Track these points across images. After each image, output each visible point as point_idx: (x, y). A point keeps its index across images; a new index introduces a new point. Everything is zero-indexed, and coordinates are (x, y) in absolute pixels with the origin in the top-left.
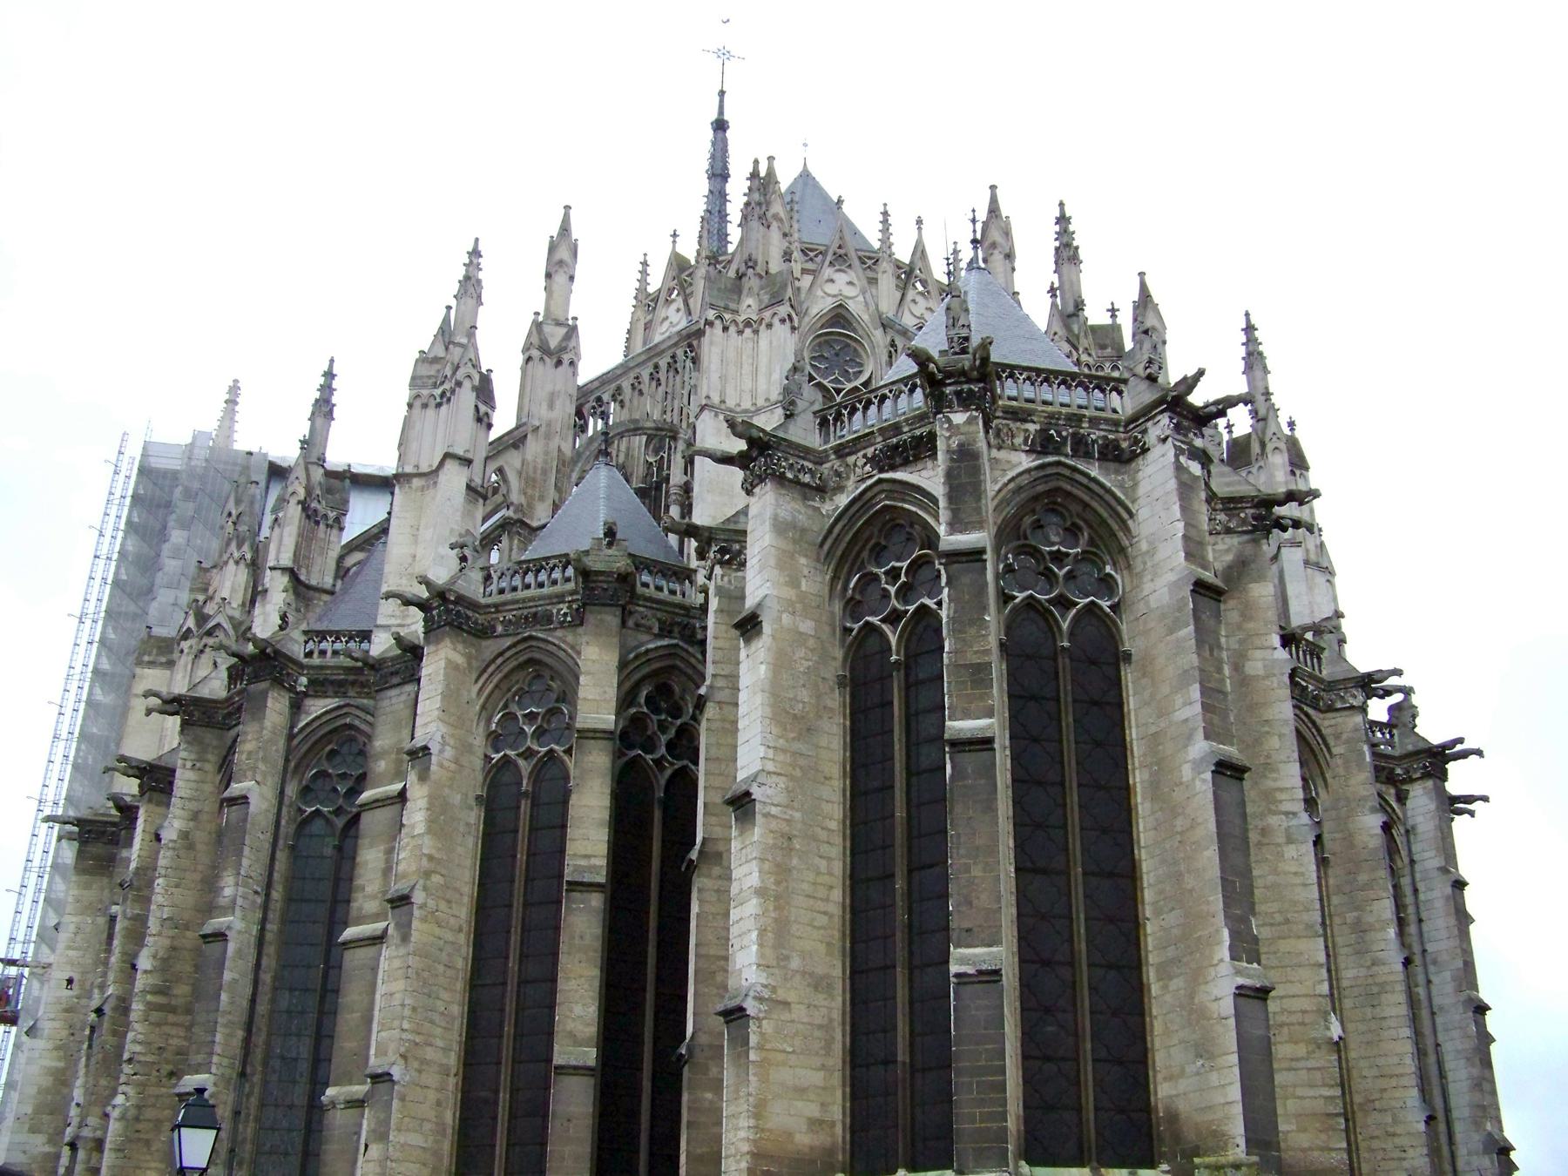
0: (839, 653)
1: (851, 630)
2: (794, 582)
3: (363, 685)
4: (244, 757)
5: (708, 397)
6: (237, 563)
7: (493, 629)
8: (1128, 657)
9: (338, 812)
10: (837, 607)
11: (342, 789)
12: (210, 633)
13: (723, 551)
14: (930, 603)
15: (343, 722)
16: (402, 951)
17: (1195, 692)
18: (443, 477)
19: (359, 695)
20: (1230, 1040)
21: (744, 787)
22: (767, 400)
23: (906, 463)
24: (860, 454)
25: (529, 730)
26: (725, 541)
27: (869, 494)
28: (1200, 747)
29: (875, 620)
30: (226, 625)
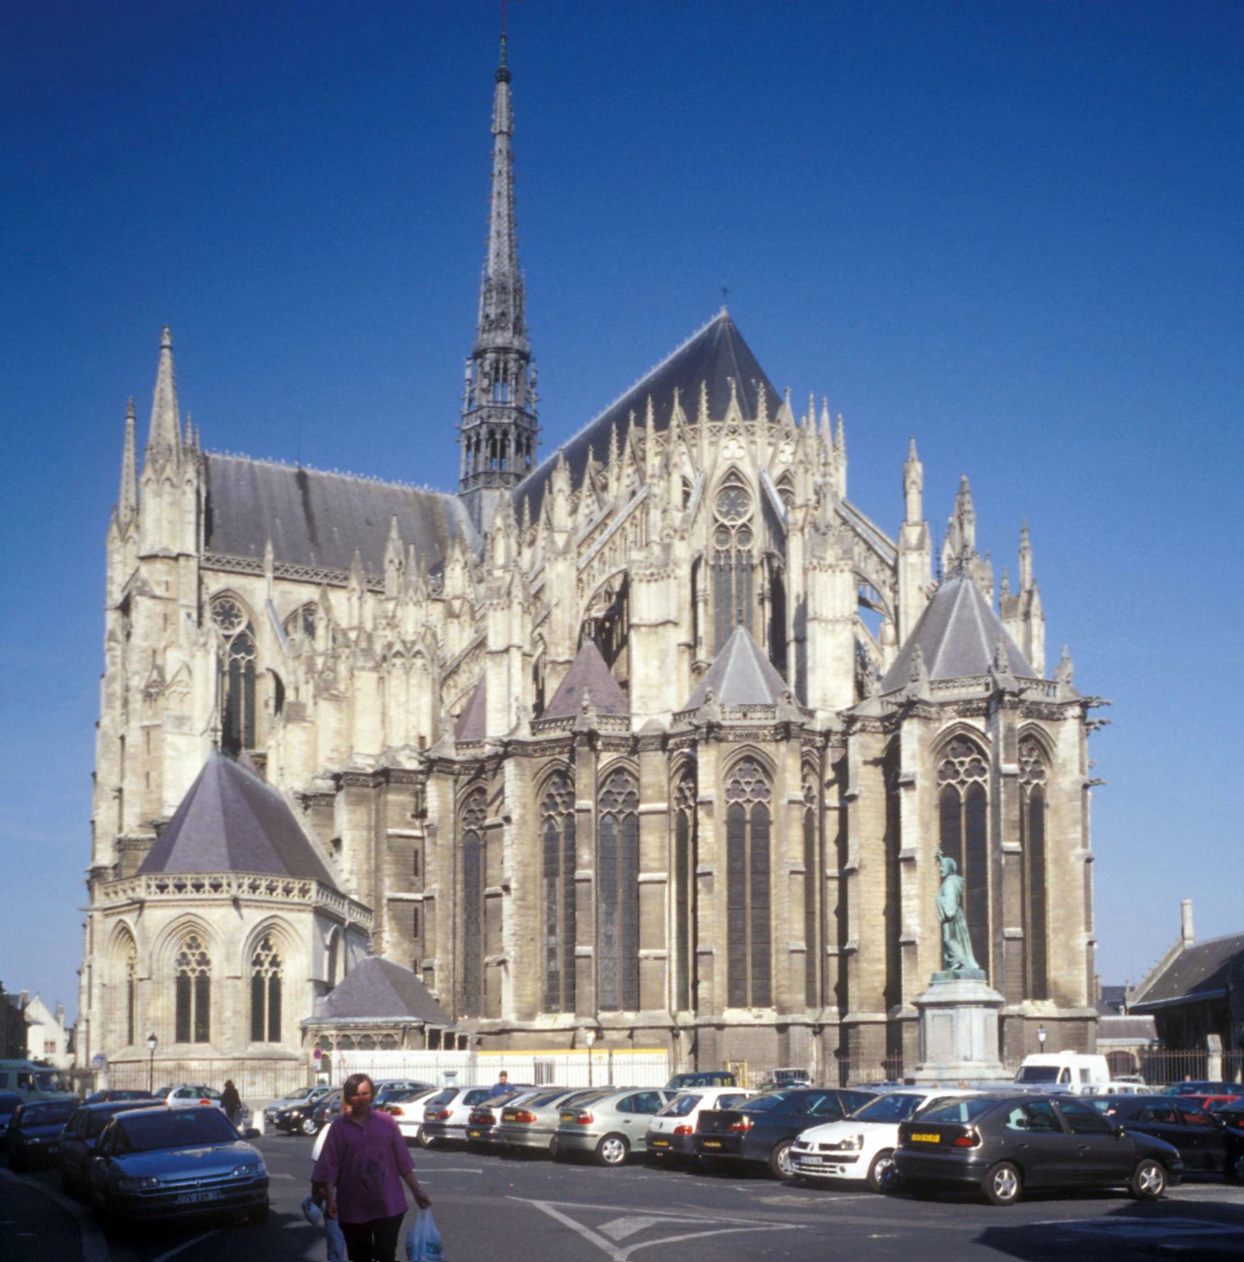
2: (923, 765)
8: (1047, 806)
12: (414, 656)
17: (1079, 828)
20: (1083, 958)
28: (1079, 850)
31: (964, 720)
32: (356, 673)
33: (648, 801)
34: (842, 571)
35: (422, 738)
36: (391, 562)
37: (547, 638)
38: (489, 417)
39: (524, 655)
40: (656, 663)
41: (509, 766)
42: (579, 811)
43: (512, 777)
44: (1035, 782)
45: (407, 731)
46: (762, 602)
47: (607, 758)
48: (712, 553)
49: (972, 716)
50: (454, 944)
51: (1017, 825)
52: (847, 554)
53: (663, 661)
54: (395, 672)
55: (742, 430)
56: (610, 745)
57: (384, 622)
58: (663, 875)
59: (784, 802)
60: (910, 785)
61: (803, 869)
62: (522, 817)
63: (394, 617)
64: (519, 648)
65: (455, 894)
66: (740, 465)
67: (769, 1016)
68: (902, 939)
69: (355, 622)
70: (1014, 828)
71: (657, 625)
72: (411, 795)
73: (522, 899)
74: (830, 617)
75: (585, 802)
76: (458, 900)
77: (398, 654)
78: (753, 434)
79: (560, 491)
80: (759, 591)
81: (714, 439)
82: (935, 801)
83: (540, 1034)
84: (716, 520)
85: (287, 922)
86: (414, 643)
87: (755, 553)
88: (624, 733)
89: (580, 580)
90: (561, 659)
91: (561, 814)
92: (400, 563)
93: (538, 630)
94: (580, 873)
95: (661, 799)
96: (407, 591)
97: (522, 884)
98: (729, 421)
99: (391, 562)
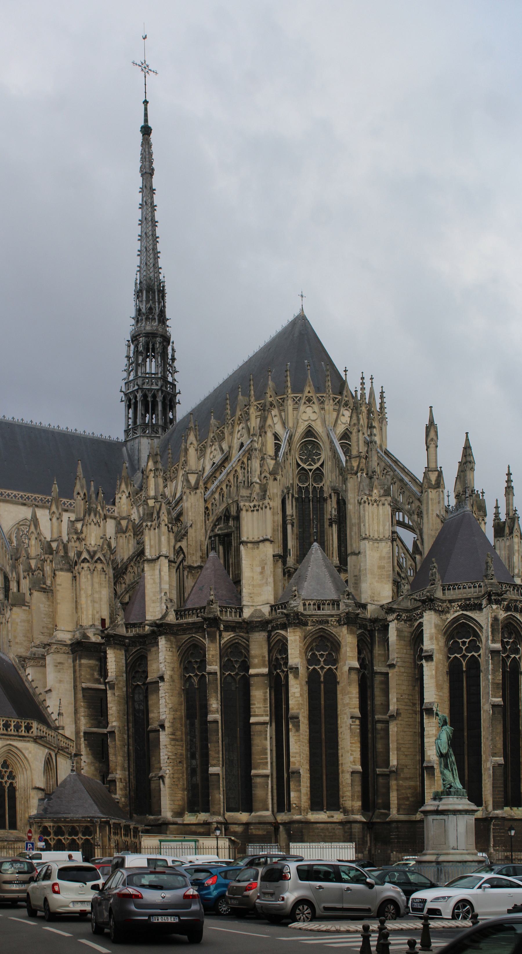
0: (447, 664)
1: (450, 657)
2: (438, 644)
3: (242, 628)
5: (366, 534)
6: (95, 524)
7: (308, 623)
9: (237, 674)
10: (446, 650)
11: (237, 666)
12: (96, 562)
13: (398, 615)
14: (476, 654)
15: (234, 642)
16: (297, 734)
19: (240, 632)
21: (430, 707)
22: (384, 537)
25: (322, 660)
26: (398, 612)
29: (458, 656)
30: (102, 558)
31: (465, 613)
32: (57, 573)
33: (255, 667)
35: (103, 621)
36: (78, 494)
37: (185, 550)
38: (143, 384)
39: (170, 561)
40: (259, 569)
41: (162, 642)
42: (210, 673)
43: (164, 649)
44: (513, 656)
45: (93, 615)
46: (331, 525)
47: (227, 636)
48: (296, 489)
49: (471, 610)
50: (129, 763)
51: (501, 686)
52: (387, 493)
53: (263, 568)
54: (83, 573)
55: (315, 400)
56: (230, 627)
57: (75, 537)
58: (267, 719)
59: (346, 668)
60: (429, 658)
61: (359, 715)
62: (171, 677)
63: (82, 532)
64: (166, 557)
65: (128, 730)
66: (313, 424)
67: (338, 816)
68: (425, 765)
69: (55, 536)
70: (498, 688)
71: (258, 542)
72: (97, 660)
73: (173, 734)
74: (376, 536)
75: (214, 667)
76: (130, 733)
77: (85, 560)
78: (323, 403)
79: (191, 444)
80: (329, 517)
81: (296, 406)
82: (446, 669)
83: (187, 827)
84: (299, 465)
85: (16, 747)
86: (95, 552)
87: (325, 489)
88: (238, 619)
89: (207, 508)
90: (195, 565)
91: (196, 675)
92: (85, 494)
93: (179, 544)
94: (211, 717)
95: (264, 666)
96: (90, 515)
97: (173, 723)
98: (306, 394)
99: (78, 494)
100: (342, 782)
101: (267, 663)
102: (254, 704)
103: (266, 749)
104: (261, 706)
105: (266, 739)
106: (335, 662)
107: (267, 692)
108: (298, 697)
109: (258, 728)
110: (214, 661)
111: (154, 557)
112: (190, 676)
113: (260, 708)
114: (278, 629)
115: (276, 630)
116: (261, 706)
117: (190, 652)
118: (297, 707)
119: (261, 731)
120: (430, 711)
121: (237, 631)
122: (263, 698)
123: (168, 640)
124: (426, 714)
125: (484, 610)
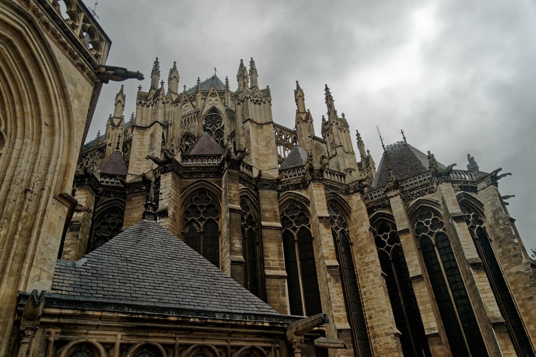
4: (232, 195)
14: (482, 226)
18: (265, 127)
23: (468, 191)
24: (457, 184)
27: (460, 195)
33: (267, 220)
34: (345, 132)
95: (276, 220)
100: (376, 349)
101: (279, 218)
102: (269, 257)
103: (286, 307)
104: (276, 259)
105: (284, 295)
106: (345, 225)
107: (281, 245)
108: (332, 246)
109: (274, 282)
110: (236, 200)
111: (144, 126)
112: (193, 221)
113: (275, 261)
114: (289, 190)
115: (285, 190)
116: (276, 259)
117: (194, 197)
118: (332, 256)
119: (278, 286)
120: (475, 266)
121: (247, 185)
122: (277, 250)
123: (174, 178)
124: (473, 269)
125: (479, 192)
